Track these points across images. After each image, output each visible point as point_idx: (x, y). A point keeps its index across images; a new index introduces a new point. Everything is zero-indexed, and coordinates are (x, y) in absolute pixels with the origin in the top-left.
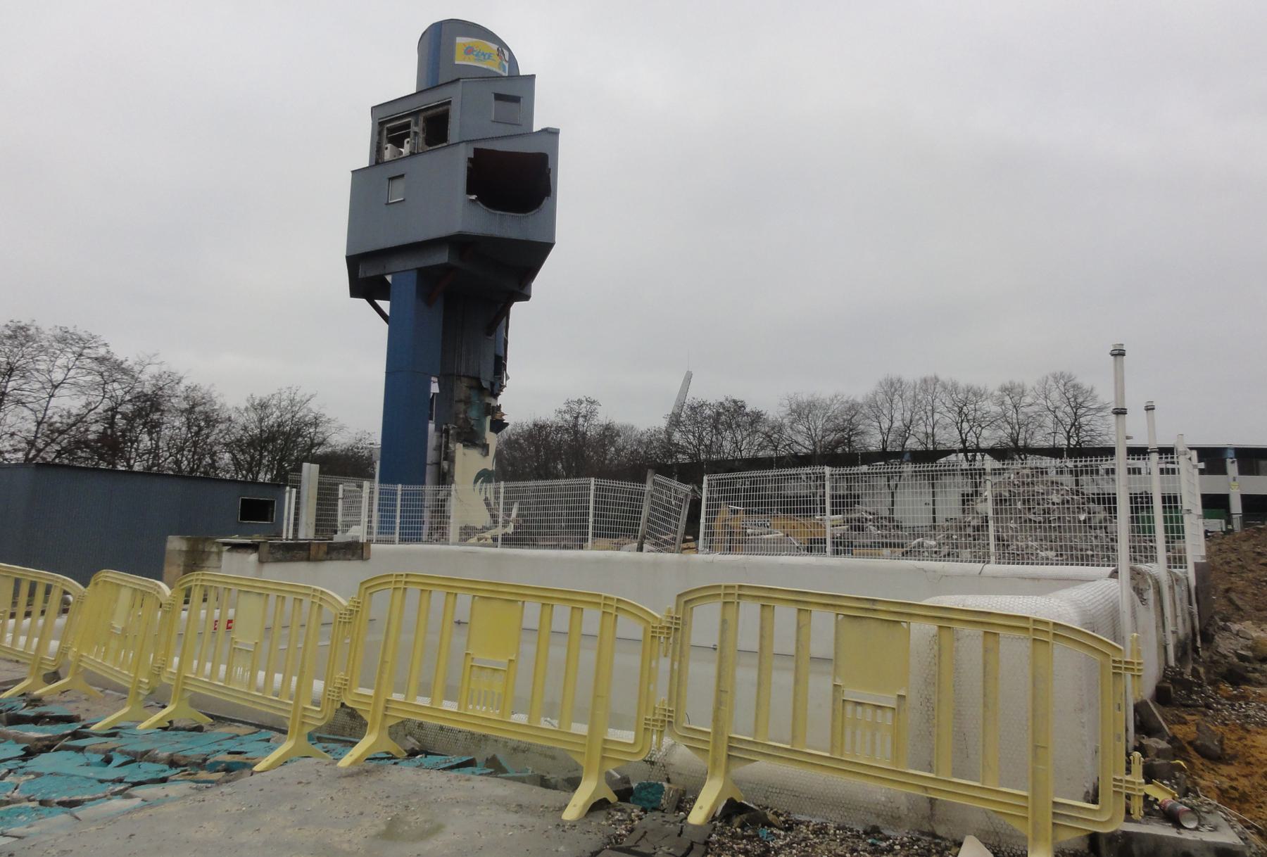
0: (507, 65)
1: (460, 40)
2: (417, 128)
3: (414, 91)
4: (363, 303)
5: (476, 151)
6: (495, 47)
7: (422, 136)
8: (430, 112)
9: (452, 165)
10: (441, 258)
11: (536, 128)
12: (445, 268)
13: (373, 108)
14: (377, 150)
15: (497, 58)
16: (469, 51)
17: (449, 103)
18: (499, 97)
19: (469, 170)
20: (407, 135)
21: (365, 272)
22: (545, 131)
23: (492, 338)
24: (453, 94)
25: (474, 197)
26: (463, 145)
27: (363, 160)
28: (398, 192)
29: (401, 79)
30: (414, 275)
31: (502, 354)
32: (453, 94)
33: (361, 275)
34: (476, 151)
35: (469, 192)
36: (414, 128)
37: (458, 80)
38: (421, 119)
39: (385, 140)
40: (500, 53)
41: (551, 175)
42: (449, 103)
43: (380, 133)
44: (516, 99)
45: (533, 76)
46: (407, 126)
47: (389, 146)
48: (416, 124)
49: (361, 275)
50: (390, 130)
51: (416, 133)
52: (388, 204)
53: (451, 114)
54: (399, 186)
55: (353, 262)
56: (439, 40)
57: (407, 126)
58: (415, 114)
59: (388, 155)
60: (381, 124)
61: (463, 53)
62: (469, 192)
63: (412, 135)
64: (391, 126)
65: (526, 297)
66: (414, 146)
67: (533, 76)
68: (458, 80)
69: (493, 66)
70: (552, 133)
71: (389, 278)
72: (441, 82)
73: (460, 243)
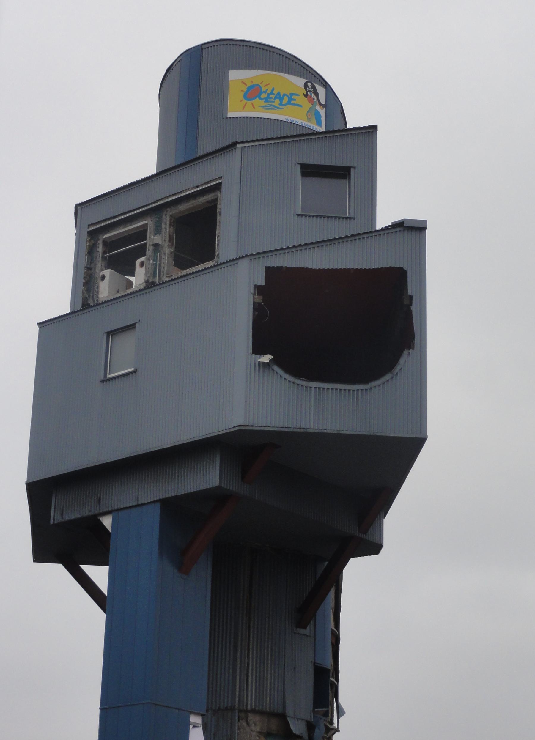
0: (322, 112)
1: (236, 76)
2: (160, 237)
3: (152, 170)
4: (57, 571)
5: (269, 271)
6: (299, 82)
7: (167, 250)
8: (183, 207)
9: (228, 297)
10: (208, 477)
11: (383, 221)
12: (216, 498)
13: (80, 208)
14: (85, 282)
15: (304, 101)
16: (253, 92)
18: (309, 171)
19: (257, 308)
20: (141, 251)
21: (66, 510)
22: (400, 226)
23: (307, 632)
24: (227, 170)
25: (266, 358)
26: (244, 264)
27: (61, 304)
28: (125, 355)
29: (130, 150)
30: (155, 512)
31: (329, 663)
33: (55, 517)
34: (269, 271)
36: (153, 238)
37: (233, 145)
38: (166, 219)
39: (99, 263)
40: (310, 92)
41: (413, 308)
42: (218, 187)
43: (91, 251)
44: (342, 173)
45: (374, 128)
46: (141, 234)
47: (107, 273)
48: (158, 231)
49: (55, 517)
50: (109, 245)
51: (156, 245)
52: (105, 380)
54: (126, 348)
55: (40, 493)
56: (196, 79)
57: (141, 234)
58: (156, 211)
59: (105, 290)
60: (93, 234)
61: (240, 98)
63: (149, 251)
64: (109, 234)
65: (374, 548)
67: (374, 128)
68: (233, 145)
69: (300, 115)
71: (107, 522)
72: (200, 153)
73: (243, 449)
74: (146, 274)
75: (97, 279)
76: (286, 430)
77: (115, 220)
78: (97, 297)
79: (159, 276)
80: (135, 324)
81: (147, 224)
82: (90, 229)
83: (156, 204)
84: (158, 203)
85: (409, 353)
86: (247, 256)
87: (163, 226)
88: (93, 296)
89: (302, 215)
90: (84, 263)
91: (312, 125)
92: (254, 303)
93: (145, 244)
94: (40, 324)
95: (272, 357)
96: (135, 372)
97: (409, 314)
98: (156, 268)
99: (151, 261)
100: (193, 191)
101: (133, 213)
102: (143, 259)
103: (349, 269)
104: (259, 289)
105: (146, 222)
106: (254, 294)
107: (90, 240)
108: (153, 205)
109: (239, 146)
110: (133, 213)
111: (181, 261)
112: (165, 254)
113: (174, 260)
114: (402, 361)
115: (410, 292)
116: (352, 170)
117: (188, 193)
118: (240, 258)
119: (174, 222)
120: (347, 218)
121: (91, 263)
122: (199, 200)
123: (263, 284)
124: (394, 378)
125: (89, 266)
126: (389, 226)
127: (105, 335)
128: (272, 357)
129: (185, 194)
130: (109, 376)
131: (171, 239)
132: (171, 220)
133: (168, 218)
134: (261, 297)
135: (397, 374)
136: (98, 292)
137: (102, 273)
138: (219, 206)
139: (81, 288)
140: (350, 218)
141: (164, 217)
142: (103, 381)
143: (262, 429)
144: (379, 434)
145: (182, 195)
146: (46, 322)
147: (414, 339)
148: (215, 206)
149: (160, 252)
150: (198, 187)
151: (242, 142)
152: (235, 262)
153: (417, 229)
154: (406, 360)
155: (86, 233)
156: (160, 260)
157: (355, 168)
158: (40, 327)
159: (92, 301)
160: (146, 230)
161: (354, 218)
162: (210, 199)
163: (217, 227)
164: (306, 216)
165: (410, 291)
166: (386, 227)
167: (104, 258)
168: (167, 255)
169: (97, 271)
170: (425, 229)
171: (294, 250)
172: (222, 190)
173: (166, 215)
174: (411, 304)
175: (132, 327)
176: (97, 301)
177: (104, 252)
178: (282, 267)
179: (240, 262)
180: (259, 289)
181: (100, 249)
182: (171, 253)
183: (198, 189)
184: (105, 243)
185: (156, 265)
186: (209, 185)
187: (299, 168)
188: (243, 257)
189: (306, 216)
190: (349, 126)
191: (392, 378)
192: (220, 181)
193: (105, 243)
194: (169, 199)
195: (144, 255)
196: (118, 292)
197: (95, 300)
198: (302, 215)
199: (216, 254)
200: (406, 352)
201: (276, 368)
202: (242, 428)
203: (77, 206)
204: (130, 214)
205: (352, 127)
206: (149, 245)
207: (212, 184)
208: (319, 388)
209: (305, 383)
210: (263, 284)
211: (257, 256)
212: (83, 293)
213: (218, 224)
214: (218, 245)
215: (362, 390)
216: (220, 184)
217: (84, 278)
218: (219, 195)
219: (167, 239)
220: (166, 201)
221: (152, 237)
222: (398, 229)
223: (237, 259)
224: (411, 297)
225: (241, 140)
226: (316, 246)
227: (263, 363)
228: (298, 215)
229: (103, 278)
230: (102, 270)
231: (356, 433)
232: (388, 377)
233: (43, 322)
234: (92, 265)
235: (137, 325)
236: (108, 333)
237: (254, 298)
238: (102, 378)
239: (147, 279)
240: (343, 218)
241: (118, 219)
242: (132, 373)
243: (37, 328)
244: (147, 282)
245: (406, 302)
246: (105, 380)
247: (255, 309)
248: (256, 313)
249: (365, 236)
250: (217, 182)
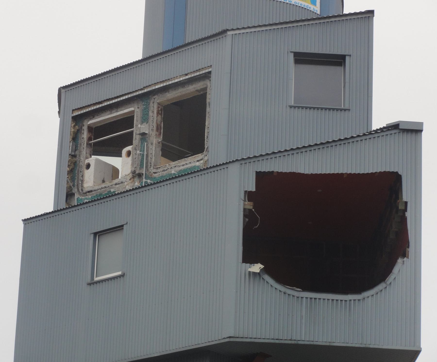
2: (147, 126)
3: (139, 56)
5: (261, 177)
7: (155, 140)
8: (171, 95)
11: (377, 123)
13: (63, 91)
14: (71, 170)
17: (207, 76)
18: (302, 58)
19: (247, 214)
20: (127, 140)
22: (394, 127)
24: (216, 58)
25: (257, 268)
26: (234, 168)
28: (113, 258)
32: (216, 58)
34: (261, 177)
35: (248, 257)
36: (139, 127)
38: (154, 106)
39: (84, 150)
41: (408, 214)
42: (207, 76)
43: (75, 138)
45: (371, 13)
46: (128, 121)
48: (145, 119)
50: (96, 131)
51: (143, 134)
52: (92, 283)
53: (211, 98)
54: (113, 245)
57: (128, 121)
58: (144, 97)
59: (90, 180)
60: (77, 120)
62: (248, 257)
63: (136, 139)
64: (95, 122)
66: (141, 162)
67: (371, 13)
70: (411, 132)
72: (188, 40)
74: (132, 165)
75: (81, 167)
76: (277, 342)
77: (101, 106)
78: (82, 186)
79: (147, 167)
80: (122, 226)
81: (133, 112)
82: (74, 114)
83: (143, 92)
84: (146, 91)
85: (404, 261)
86: (237, 160)
87: (151, 114)
88: (77, 185)
89: (295, 107)
90: (68, 150)
91: (306, 4)
92: (245, 209)
93: (132, 132)
94: (24, 220)
95: (262, 267)
96: (123, 276)
97: (403, 221)
98: (143, 158)
99: (138, 152)
100: (181, 79)
101: (119, 99)
102: (129, 148)
103: (342, 174)
104: (249, 195)
105: (132, 109)
106: (245, 201)
107: (74, 126)
108: (140, 92)
109: (229, 33)
110: (119, 99)
111: (170, 153)
112: (152, 144)
113: (162, 150)
114: (396, 270)
115: (405, 199)
116: (347, 58)
117: (176, 81)
118: (230, 162)
119: (161, 110)
120: (341, 110)
121: (75, 150)
122: (188, 88)
123: (254, 190)
124: (388, 287)
125: (73, 153)
126: (384, 128)
127: (92, 236)
128: (262, 267)
129: (173, 82)
130: (96, 279)
131: (158, 128)
132: (158, 107)
133: (156, 106)
134: (252, 203)
135: (390, 283)
136: (82, 181)
137: (87, 161)
138: (208, 96)
139: (65, 176)
140: (345, 110)
141: (151, 104)
142: (90, 284)
143: (252, 340)
144: (371, 346)
145: (170, 83)
146: (31, 218)
147: (408, 247)
148: (205, 94)
149: (147, 142)
150: (186, 75)
151: (233, 30)
152: (225, 166)
153: (414, 131)
154: (401, 267)
155: (71, 119)
156: (147, 151)
157: (350, 56)
158: (25, 224)
159: (76, 190)
160: (133, 117)
161: (349, 110)
162: (199, 88)
163: (207, 118)
164: (299, 107)
165: (406, 196)
166: (381, 129)
167: (89, 145)
168: (154, 145)
169: (82, 159)
170: (421, 131)
171: (286, 154)
172: (211, 79)
173: (153, 103)
174: (406, 210)
175: (120, 228)
176: (82, 190)
177: (90, 139)
178: (273, 172)
179: (230, 166)
180: (249, 195)
181: (85, 135)
182: (159, 143)
183: (187, 77)
184: (90, 129)
185: (143, 155)
186: (198, 74)
187: (292, 55)
188: (233, 161)
189: (299, 107)
190: (346, 12)
191: (386, 287)
192: (210, 70)
193: (90, 129)
194: (157, 87)
195: (131, 144)
196: (104, 181)
197: (80, 189)
198: (295, 107)
199: (206, 147)
200: (400, 261)
201: (267, 278)
202: (232, 340)
203: (60, 90)
204: (116, 100)
205: (347, 13)
206: (136, 134)
207: (201, 73)
208: (311, 298)
209: (296, 294)
210: (254, 190)
211: (247, 161)
212: (68, 182)
213: (208, 105)
214: (207, 137)
215: (354, 300)
216: (210, 73)
217: (69, 166)
218: (208, 84)
219: (155, 128)
220: (154, 88)
221: (139, 126)
222: (393, 132)
223: (227, 163)
224: (406, 203)
225: (231, 28)
226: (308, 149)
227: (253, 272)
228: (291, 107)
229: (88, 166)
230: (87, 158)
231: (348, 345)
232: (381, 286)
233: (28, 219)
234: (77, 152)
235: (125, 227)
236: (95, 234)
237: (244, 205)
238: (89, 281)
239: (133, 169)
240: (337, 110)
241: (103, 105)
242: (120, 276)
243: (22, 225)
244: (134, 172)
245: (401, 207)
246: (92, 283)
247: (245, 216)
248: (247, 220)
249: (359, 139)
250: (207, 71)
